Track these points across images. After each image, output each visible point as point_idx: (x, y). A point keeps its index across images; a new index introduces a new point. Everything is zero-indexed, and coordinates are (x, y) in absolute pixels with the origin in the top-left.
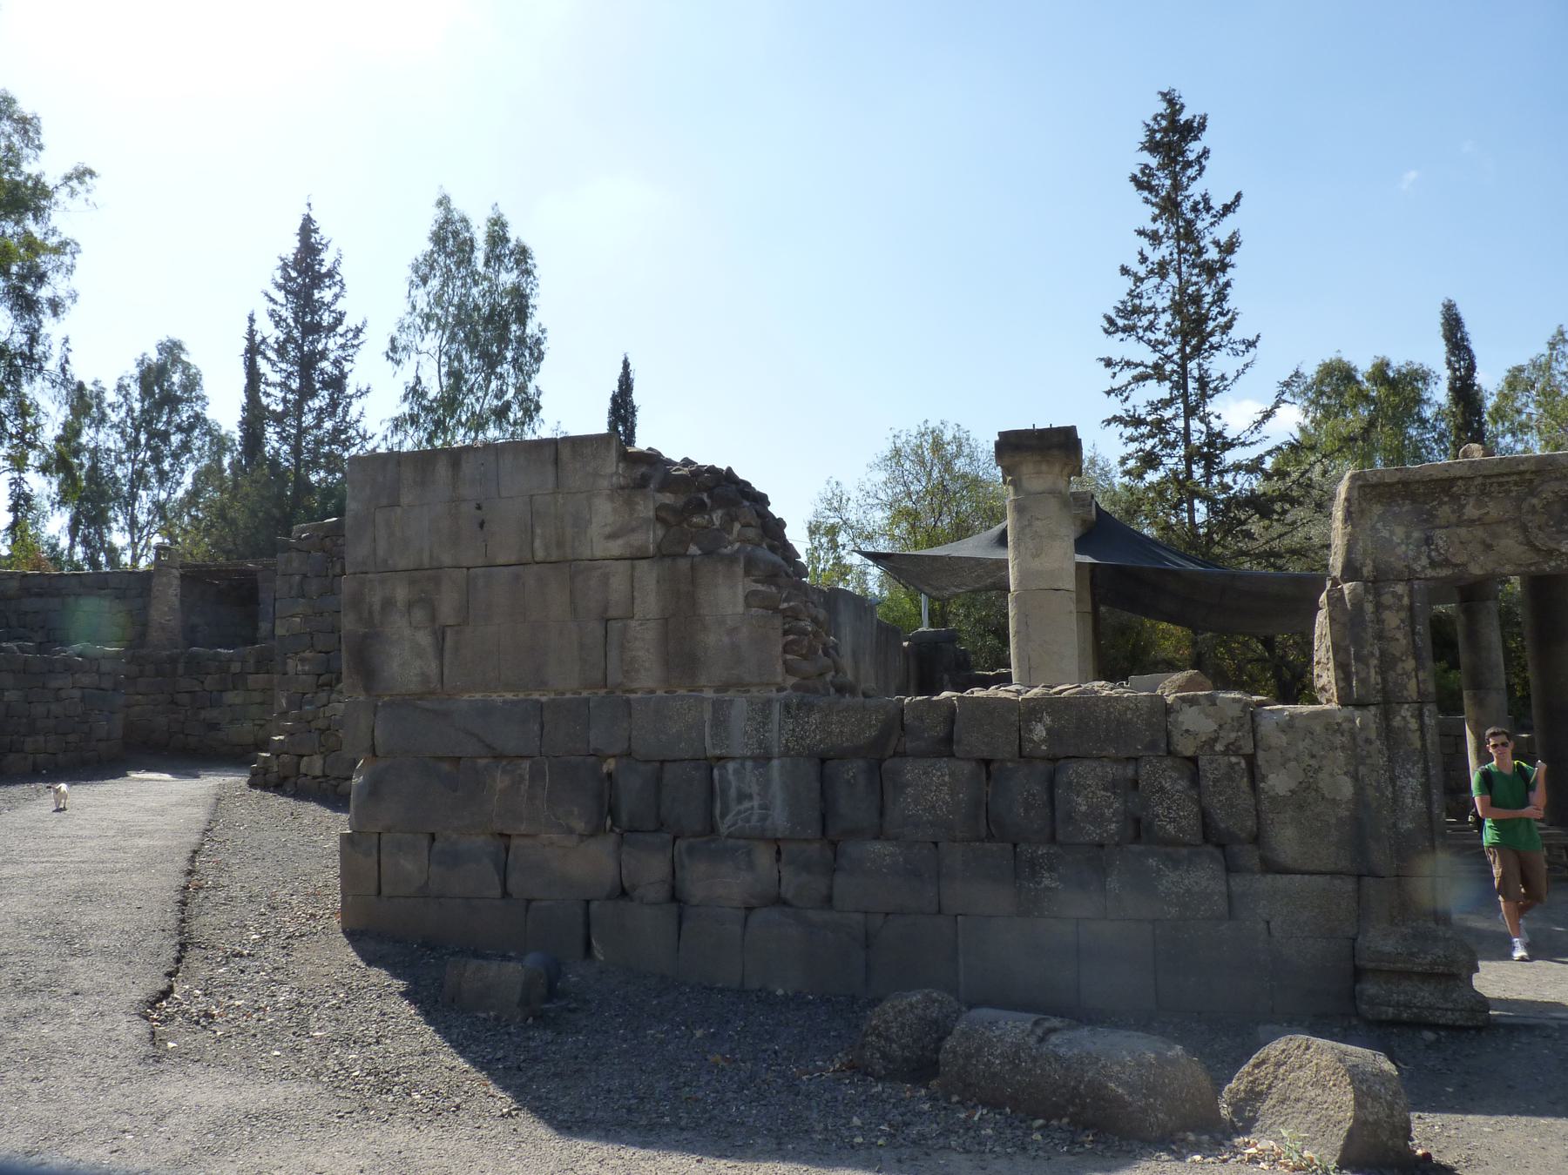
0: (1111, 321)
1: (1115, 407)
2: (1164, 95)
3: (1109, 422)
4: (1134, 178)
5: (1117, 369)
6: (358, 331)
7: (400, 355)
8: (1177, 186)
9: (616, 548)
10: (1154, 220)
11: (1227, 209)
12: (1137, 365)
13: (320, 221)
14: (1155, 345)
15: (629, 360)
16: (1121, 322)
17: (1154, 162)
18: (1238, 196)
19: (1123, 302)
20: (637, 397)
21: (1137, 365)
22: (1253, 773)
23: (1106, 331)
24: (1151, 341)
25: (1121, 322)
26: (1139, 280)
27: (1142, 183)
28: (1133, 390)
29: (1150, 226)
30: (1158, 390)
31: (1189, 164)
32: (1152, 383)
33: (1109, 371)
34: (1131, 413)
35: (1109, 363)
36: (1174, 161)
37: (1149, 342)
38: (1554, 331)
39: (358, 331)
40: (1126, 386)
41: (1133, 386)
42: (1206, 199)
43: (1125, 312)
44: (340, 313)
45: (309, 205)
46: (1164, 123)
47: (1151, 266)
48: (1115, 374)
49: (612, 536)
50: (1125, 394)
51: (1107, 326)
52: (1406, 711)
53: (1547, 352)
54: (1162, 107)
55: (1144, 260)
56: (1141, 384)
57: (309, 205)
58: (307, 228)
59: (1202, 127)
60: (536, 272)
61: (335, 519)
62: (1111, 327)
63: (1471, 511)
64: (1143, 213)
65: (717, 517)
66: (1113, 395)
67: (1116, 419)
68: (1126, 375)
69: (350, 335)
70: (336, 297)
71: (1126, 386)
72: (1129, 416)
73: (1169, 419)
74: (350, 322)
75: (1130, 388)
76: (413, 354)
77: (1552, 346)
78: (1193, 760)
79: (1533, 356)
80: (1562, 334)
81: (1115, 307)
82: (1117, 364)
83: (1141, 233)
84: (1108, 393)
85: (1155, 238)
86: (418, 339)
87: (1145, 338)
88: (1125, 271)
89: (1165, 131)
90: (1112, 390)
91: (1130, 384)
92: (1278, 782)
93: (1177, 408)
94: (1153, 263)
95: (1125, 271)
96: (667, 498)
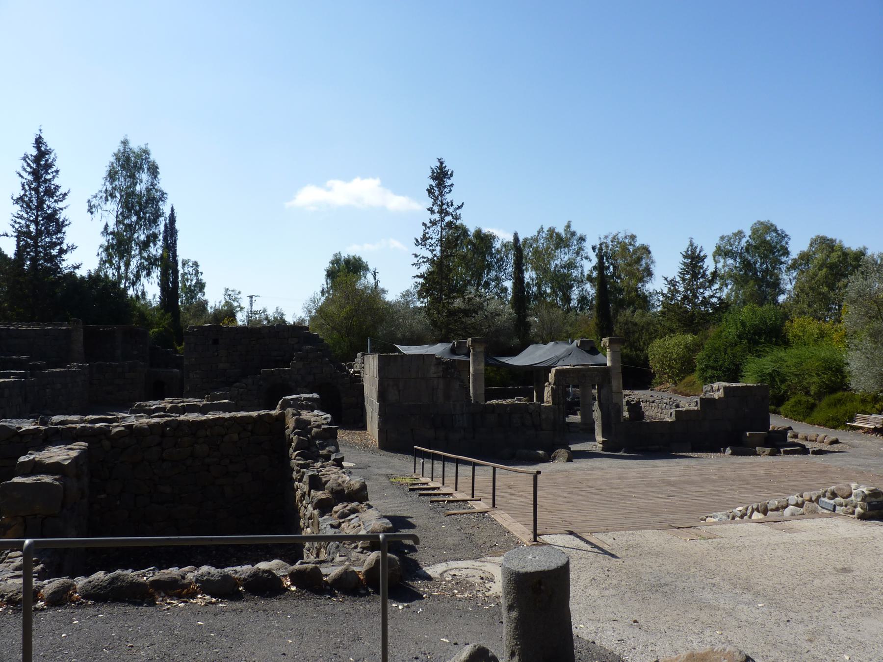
0: (417, 240)
2: (439, 160)
3: (415, 277)
4: (428, 190)
6: (66, 194)
7: (94, 210)
8: (441, 194)
9: (435, 376)
11: (459, 207)
12: (425, 258)
13: (46, 138)
15: (174, 208)
18: (463, 203)
20: (178, 226)
21: (425, 258)
22: (540, 415)
23: (416, 244)
27: (430, 191)
31: (445, 187)
35: (416, 256)
36: (441, 185)
37: (430, 250)
38: (540, 227)
39: (66, 194)
42: (452, 203)
44: (57, 186)
45: (40, 130)
49: (434, 374)
52: (561, 406)
53: (537, 235)
54: (438, 164)
57: (40, 130)
58: (39, 142)
59: (451, 175)
61: (209, 325)
62: (417, 243)
63: (572, 375)
64: (429, 202)
65: (453, 370)
69: (61, 196)
70: (54, 177)
74: (62, 191)
76: (99, 210)
77: (539, 232)
78: (531, 413)
79: (532, 235)
80: (542, 229)
84: (413, 265)
86: (103, 203)
90: (415, 264)
92: (543, 416)
96: (444, 366)
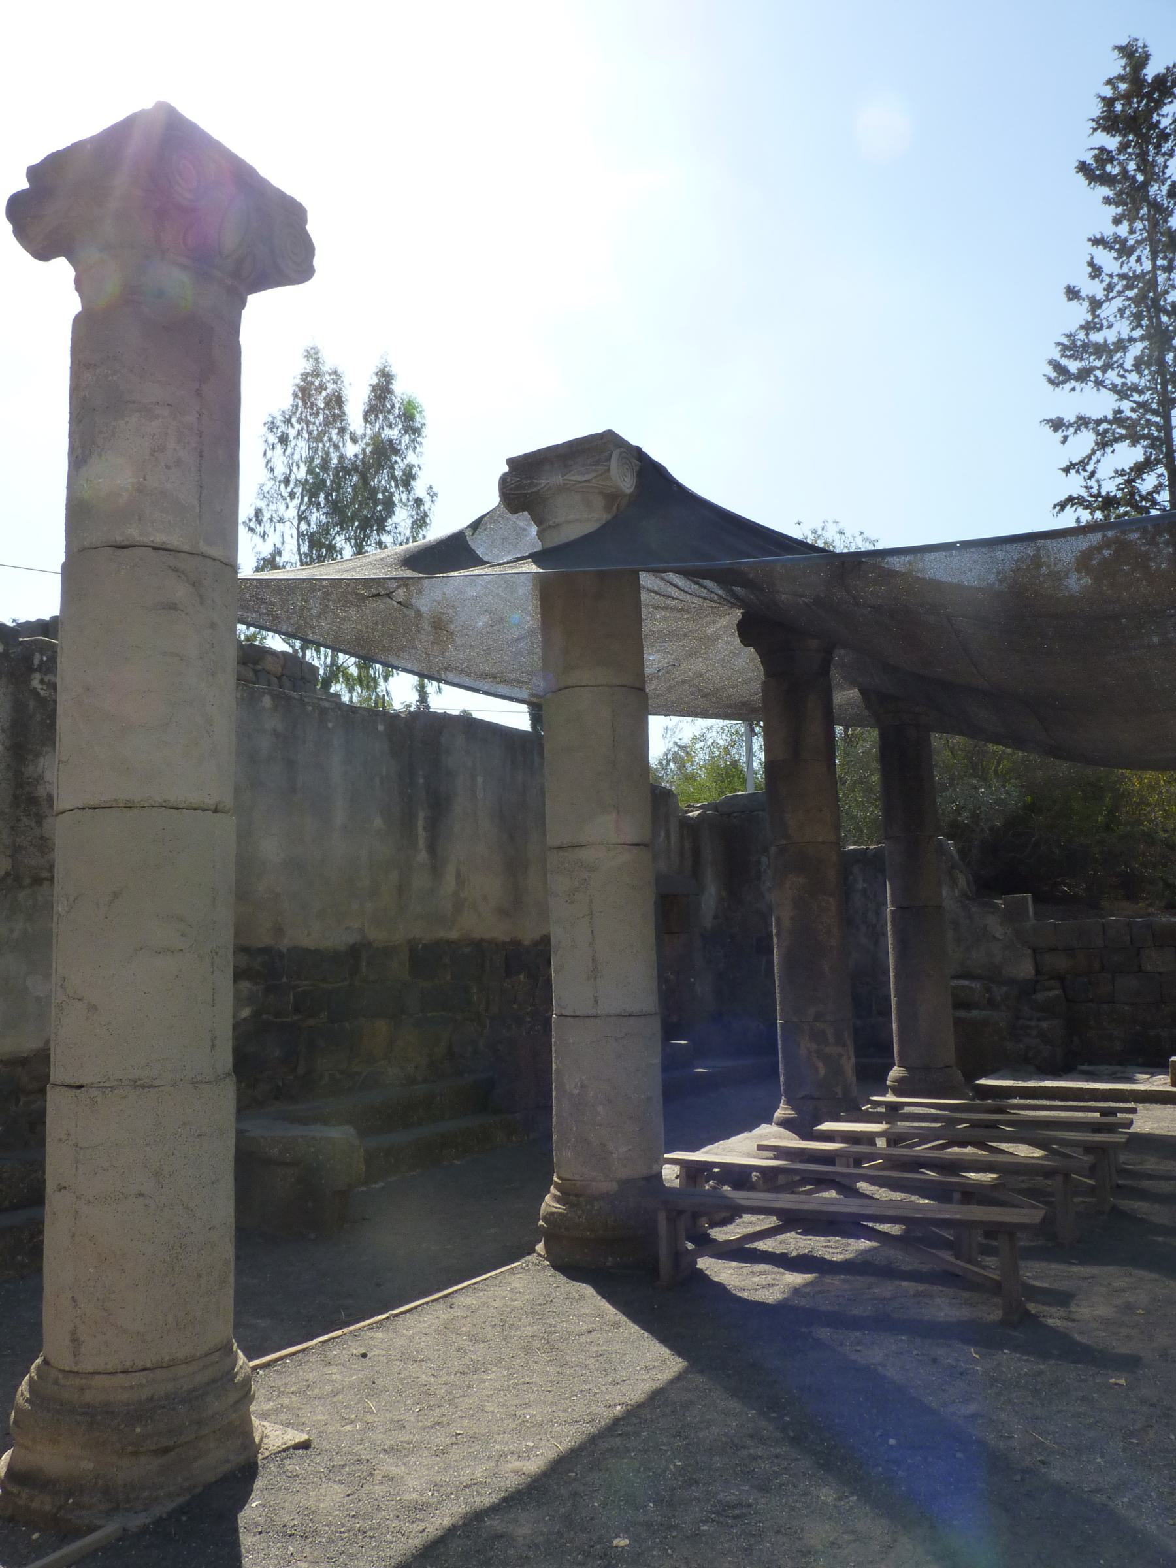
1: (1075, 485)
4: (1083, 167)
5: (1072, 430)
10: (1117, 221)
14: (1123, 392)
16: (1073, 366)
17: (1112, 142)
19: (1069, 336)
23: (1052, 382)
24: (1117, 386)
25: (1073, 366)
26: (1095, 304)
28: (1099, 461)
29: (1109, 230)
30: (1127, 455)
32: (1122, 447)
33: (1059, 435)
34: (1095, 491)
35: (1057, 425)
37: (1114, 388)
40: (1089, 457)
41: (1099, 454)
43: (1072, 348)
46: (1123, 86)
47: (1107, 279)
48: (1065, 438)
50: (1090, 468)
51: (1053, 375)
55: (1096, 271)
56: (1109, 450)
60: (425, 432)
66: (1073, 472)
67: (1070, 500)
68: (1085, 441)
71: (1089, 457)
72: (1091, 496)
73: (1150, 493)
75: (1094, 459)
81: (1058, 344)
82: (1071, 425)
83: (1097, 242)
84: (1066, 470)
85: (1123, 250)
87: (1107, 382)
88: (1072, 293)
89: (1127, 97)
91: (1094, 452)
93: (1161, 475)
94: (1111, 276)
95: (1072, 293)
